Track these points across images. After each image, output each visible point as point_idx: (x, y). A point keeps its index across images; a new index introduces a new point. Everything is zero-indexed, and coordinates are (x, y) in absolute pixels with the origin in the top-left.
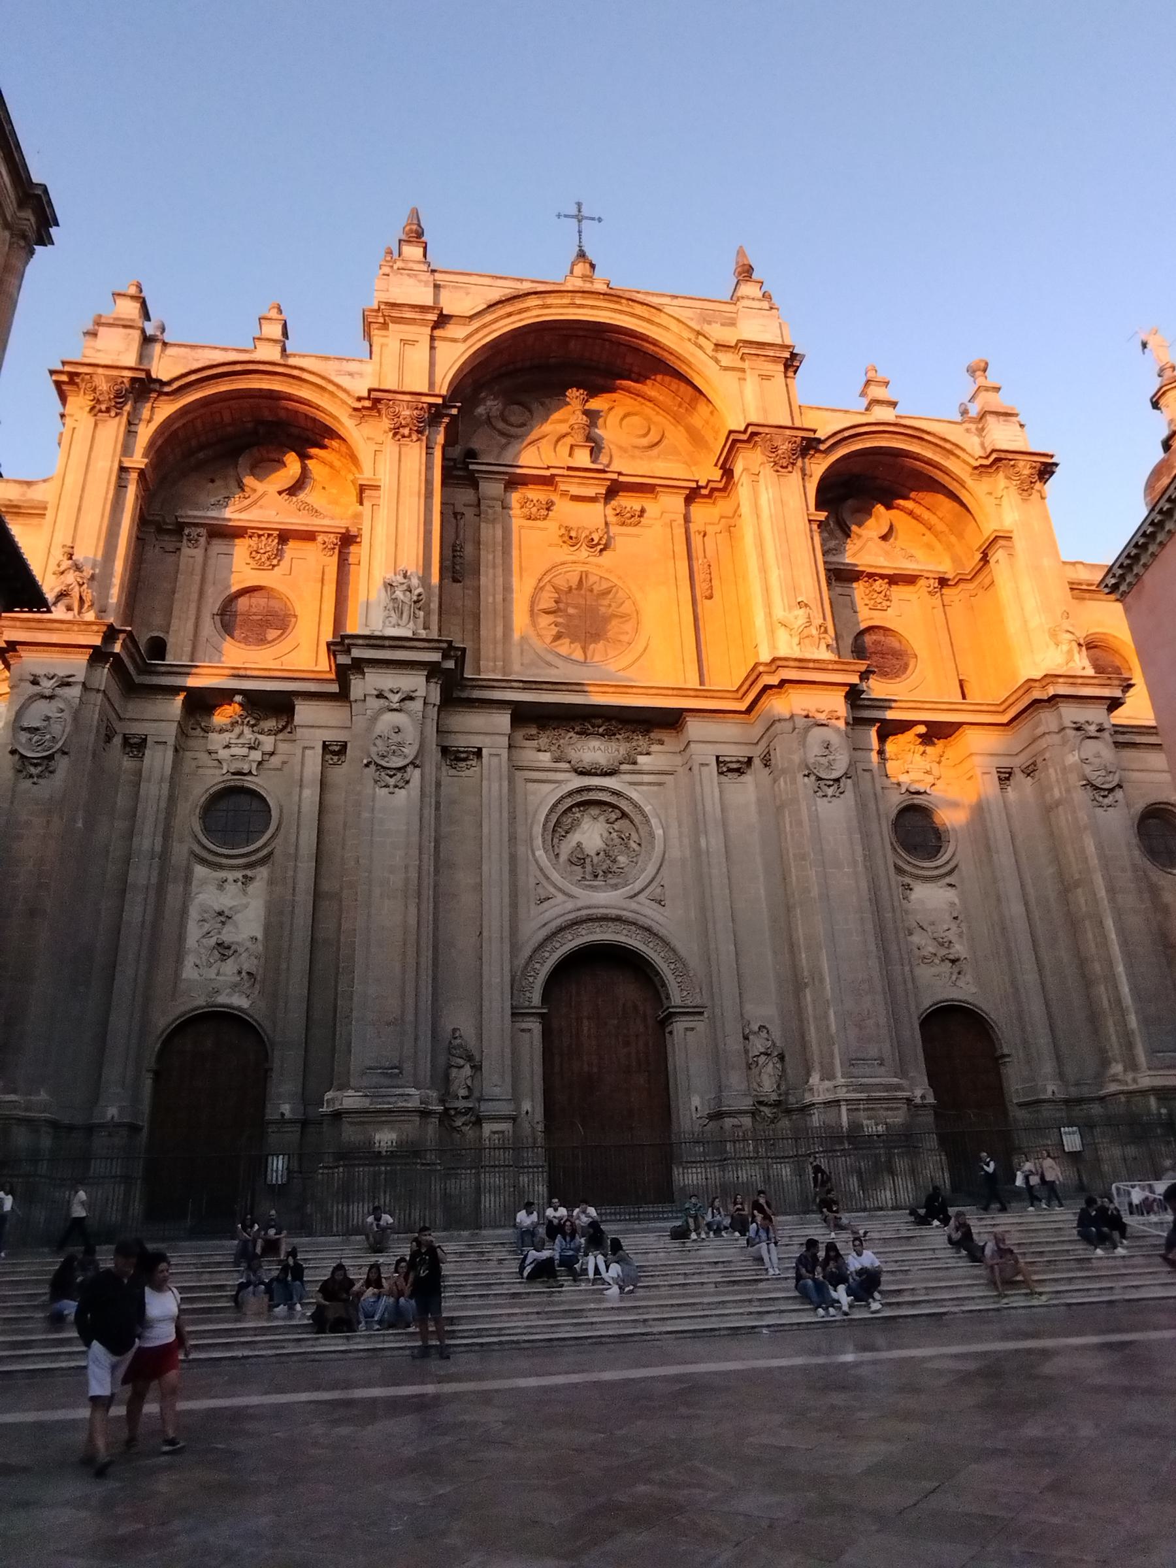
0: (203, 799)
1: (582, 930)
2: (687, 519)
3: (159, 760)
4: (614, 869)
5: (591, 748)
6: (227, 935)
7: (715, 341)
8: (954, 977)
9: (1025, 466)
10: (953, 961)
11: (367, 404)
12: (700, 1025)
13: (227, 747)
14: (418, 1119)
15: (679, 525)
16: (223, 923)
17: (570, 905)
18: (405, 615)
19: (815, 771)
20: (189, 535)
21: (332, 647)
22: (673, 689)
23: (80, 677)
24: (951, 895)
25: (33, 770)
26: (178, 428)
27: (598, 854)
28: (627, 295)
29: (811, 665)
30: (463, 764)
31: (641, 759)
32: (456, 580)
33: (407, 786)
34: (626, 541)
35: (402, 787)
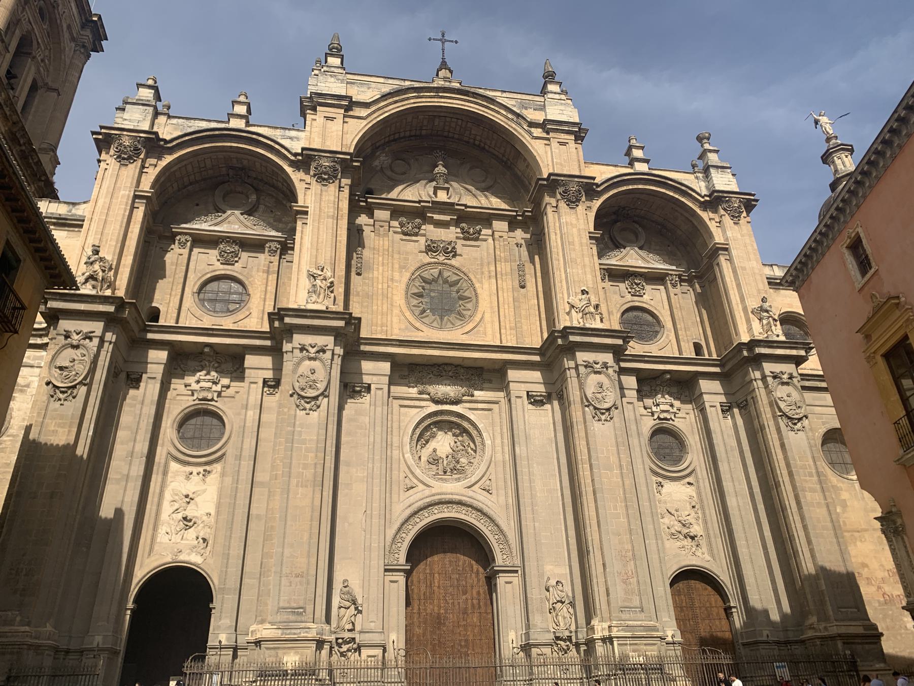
0: (180, 416)
1: (435, 509)
3: (149, 389)
4: (458, 466)
6: (190, 512)
8: (694, 549)
9: (736, 201)
10: (693, 538)
11: (300, 158)
12: (516, 580)
13: (198, 382)
14: (315, 645)
16: (189, 503)
17: (428, 492)
18: (322, 296)
19: (593, 403)
20: (179, 240)
23: (99, 332)
24: (691, 491)
25: (62, 396)
26: (174, 172)
27: (447, 457)
28: (473, 90)
31: (477, 393)
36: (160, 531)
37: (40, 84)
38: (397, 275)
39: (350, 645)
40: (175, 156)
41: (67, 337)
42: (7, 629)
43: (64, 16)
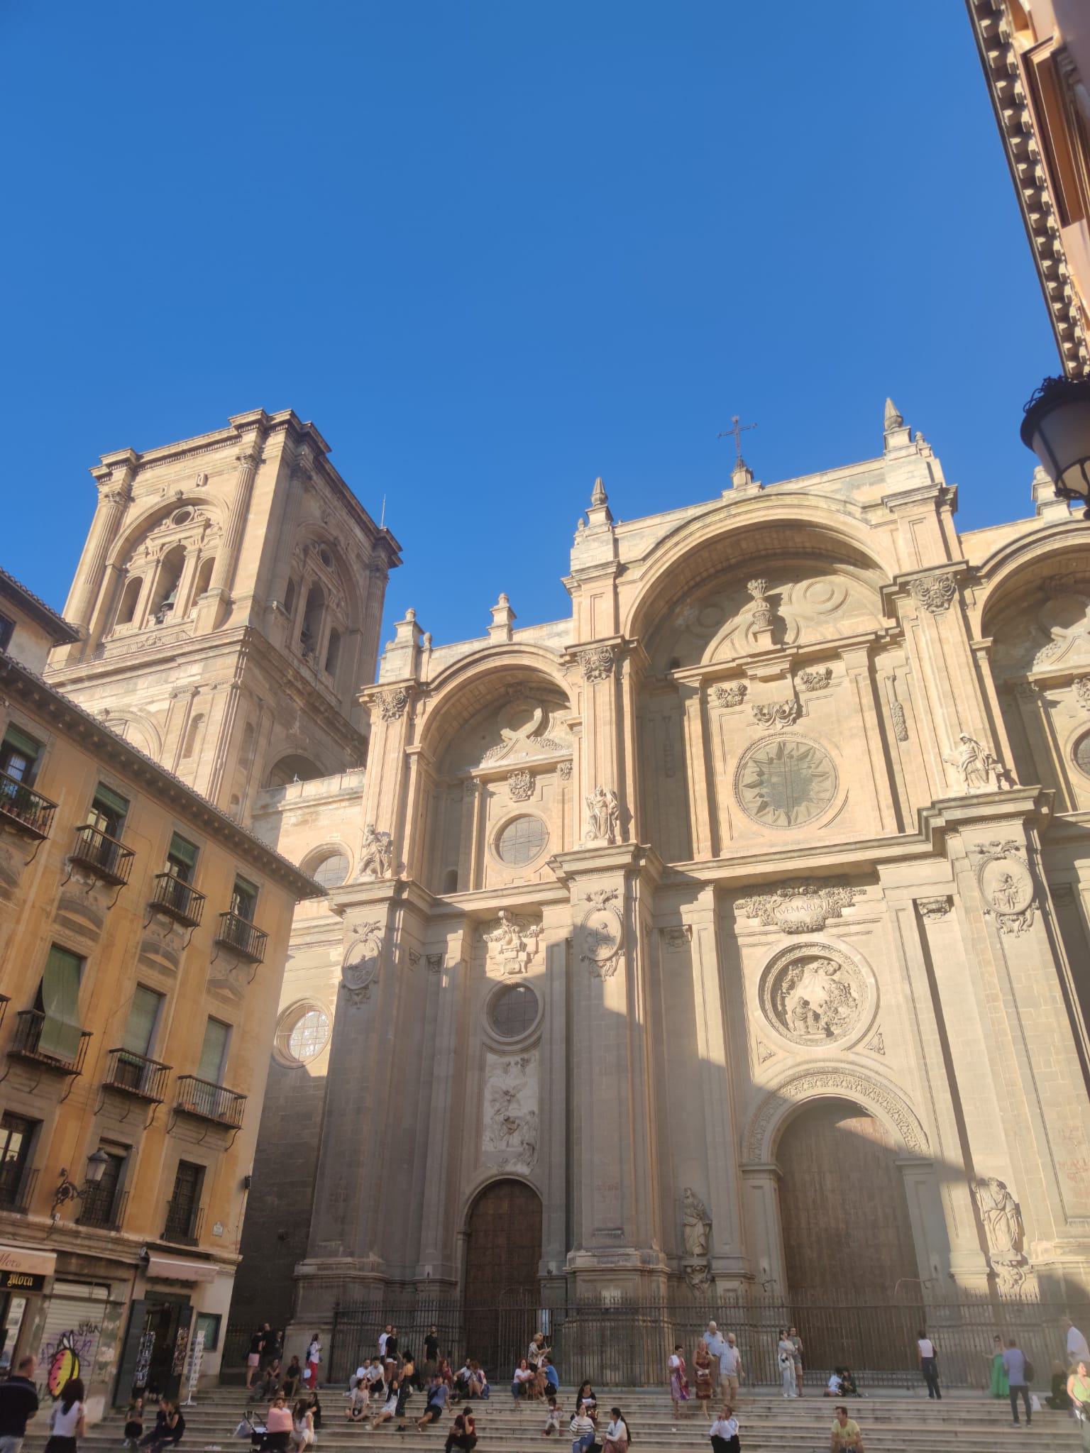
0: (488, 999)
2: (872, 670)
4: (836, 1021)
5: (795, 908)
6: (514, 1111)
7: (861, 505)
11: (567, 658)
13: (502, 952)
15: (864, 678)
17: (790, 1062)
21: (551, 865)
22: (856, 843)
23: (383, 923)
25: (356, 998)
27: (821, 1006)
29: (975, 801)
30: (679, 941)
31: (845, 911)
32: (668, 776)
33: (615, 974)
34: (816, 704)
36: (484, 1137)
37: (341, 629)
38: (718, 765)
39: (704, 1275)
41: (356, 931)
42: (332, 1260)
43: (349, 549)
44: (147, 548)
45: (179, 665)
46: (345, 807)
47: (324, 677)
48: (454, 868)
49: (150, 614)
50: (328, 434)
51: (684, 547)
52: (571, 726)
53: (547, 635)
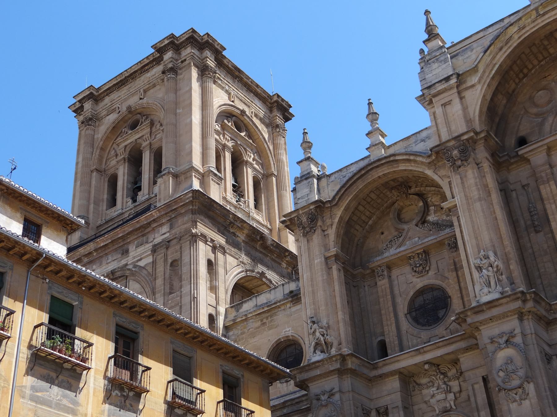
11: (434, 158)
13: (433, 396)
23: (337, 389)
26: (350, 218)
32: (537, 232)
35: (525, 399)
40: (342, 209)
41: (318, 399)
44: (116, 151)
45: (153, 229)
46: (290, 308)
47: (254, 214)
48: (382, 338)
49: (126, 198)
50: (220, 38)
51: (507, 49)
52: (450, 210)
53: (415, 142)
